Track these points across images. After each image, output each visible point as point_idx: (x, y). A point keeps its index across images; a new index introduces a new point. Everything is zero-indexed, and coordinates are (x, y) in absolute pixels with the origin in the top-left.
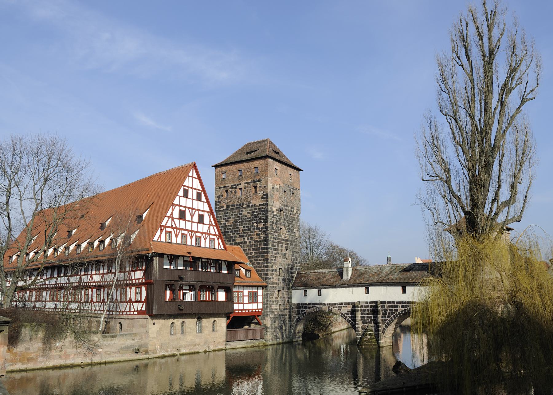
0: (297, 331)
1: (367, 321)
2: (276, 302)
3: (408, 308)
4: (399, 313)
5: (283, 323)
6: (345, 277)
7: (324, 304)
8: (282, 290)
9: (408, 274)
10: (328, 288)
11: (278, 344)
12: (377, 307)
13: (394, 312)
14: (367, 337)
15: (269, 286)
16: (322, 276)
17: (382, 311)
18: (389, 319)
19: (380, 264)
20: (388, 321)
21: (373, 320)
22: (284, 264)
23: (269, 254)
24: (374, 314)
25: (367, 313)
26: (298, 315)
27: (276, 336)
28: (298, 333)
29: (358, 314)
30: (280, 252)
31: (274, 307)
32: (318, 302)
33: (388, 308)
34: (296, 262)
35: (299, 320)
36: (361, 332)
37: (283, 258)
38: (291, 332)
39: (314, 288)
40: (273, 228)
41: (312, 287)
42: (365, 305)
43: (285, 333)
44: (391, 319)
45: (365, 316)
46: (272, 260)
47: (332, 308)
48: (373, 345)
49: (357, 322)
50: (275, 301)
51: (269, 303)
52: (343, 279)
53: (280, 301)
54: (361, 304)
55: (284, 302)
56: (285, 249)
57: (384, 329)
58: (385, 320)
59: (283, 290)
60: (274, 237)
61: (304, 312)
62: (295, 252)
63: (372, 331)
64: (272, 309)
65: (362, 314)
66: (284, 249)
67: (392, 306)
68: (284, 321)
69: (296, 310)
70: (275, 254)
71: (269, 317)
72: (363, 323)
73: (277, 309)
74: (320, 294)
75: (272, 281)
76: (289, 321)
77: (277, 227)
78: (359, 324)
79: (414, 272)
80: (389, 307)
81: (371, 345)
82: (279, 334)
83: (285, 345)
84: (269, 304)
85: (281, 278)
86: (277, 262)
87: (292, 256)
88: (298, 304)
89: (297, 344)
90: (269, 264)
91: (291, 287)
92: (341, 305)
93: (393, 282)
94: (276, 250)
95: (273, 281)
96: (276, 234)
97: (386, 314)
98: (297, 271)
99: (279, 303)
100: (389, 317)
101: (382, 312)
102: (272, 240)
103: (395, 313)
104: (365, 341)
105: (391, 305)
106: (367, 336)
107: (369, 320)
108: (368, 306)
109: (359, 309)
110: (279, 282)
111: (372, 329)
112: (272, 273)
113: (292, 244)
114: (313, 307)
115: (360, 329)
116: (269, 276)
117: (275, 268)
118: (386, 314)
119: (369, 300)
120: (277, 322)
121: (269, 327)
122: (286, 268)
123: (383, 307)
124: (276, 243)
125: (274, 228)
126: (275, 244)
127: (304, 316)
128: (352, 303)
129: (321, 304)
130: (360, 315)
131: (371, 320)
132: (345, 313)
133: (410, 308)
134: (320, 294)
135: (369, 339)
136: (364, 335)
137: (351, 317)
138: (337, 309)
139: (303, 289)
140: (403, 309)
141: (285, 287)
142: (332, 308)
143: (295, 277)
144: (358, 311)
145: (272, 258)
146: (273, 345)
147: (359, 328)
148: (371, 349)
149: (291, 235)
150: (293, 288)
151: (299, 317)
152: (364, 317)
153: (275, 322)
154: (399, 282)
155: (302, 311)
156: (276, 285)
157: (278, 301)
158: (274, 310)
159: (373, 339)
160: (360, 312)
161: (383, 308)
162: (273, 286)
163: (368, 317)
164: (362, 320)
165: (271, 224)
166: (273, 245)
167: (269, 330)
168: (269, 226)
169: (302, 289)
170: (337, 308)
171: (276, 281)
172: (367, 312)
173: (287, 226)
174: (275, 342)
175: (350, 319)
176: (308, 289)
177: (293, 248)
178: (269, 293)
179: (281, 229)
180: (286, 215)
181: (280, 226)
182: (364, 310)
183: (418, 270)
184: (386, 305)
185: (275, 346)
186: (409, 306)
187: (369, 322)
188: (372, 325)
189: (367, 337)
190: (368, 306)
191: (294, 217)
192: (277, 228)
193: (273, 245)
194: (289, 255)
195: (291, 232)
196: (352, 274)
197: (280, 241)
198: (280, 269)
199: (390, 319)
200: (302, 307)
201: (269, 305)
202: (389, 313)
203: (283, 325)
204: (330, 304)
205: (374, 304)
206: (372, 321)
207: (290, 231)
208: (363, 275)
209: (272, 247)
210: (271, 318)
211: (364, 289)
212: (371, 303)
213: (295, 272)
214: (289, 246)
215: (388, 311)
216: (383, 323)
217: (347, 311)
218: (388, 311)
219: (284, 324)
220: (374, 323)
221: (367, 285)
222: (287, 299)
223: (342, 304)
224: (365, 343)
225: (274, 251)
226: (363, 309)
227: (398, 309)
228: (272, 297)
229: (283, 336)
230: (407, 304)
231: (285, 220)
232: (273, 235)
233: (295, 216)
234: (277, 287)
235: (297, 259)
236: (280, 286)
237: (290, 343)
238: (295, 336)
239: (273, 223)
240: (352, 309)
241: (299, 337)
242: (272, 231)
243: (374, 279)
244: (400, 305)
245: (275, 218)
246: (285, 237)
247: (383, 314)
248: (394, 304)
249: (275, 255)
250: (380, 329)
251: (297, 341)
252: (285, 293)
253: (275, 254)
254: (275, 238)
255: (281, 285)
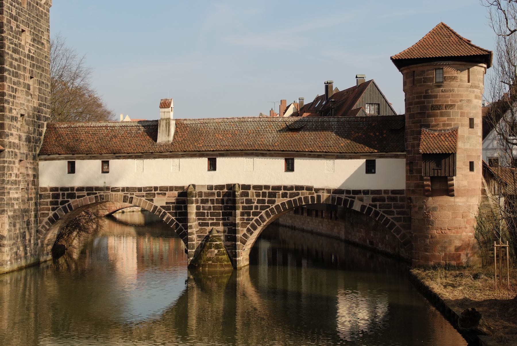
0: (46, 242)
1: (210, 222)
2: (16, 184)
3: (297, 198)
4: (277, 207)
5: (26, 226)
6: (163, 138)
7: (114, 190)
8: (25, 159)
9: (297, 135)
10: (125, 157)
11: (20, 269)
12: (235, 196)
13: (266, 204)
14: (211, 252)
15: (6, 150)
16: (107, 135)
17: (243, 203)
18: (255, 218)
19: (235, 117)
20: (253, 221)
21: (223, 219)
22: (27, 106)
23: (5, 83)
24: (225, 208)
25: (210, 207)
26: (53, 209)
27: (16, 253)
28: (48, 245)
29: (192, 209)
30: (22, 81)
31: (14, 194)
32: (100, 184)
33: (255, 197)
34: (45, 105)
35: (53, 221)
36: (195, 241)
37: (28, 94)
38: (38, 244)
39: (91, 158)
40: (11, 28)
41: (90, 155)
42: (206, 190)
43: (30, 245)
44: (261, 217)
45: (206, 211)
46: (10, 95)
47: (134, 196)
48: (226, 265)
49: (189, 224)
50: (15, 183)
51: (5, 186)
52: (158, 141)
53: (22, 183)
54: (197, 190)
55: (28, 185)
56: (29, 75)
57: (244, 235)
58: (248, 220)
59: (27, 159)
60: (13, 48)
61: (67, 204)
62: (43, 83)
63: (220, 240)
64: (10, 199)
65: (198, 208)
66: (28, 75)
67: (264, 195)
68: (28, 223)
69: (49, 200)
70: (14, 83)
71: (6, 215)
72: (200, 224)
73: (17, 199)
74: (105, 171)
75: (10, 140)
76: (34, 221)
77: (18, 26)
78: (193, 226)
79: (307, 133)
80: (258, 195)
81: (222, 266)
82: (21, 248)
83: (29, 270)
84: (6, 188)
85: (24, 136)
86: (17, 101)
87: (40, 89)
88: (53, 189)
89: (45, 266)
90: (6, 105)
91: (39, 155)
92: (153, 192)
93: (269, 150)
94: (16, 75)
95: (12, 141)
96: (15, 41)
97: (251, 208)
98: (45, 123)
99: (21, 187)
100: (255, 214)
101: (241, 205)
102: (10, 52)
103: (269, 207)
104: (209, 259)
105: (261, 192)
106: (213, 249)
107: (213, 219)
108: (213, 194)
109: (194, 198)
110: (21, 143)
111: (220, 236)
112: (10, 123)
113: (40, 67)
114: (88, 194)
115: (195, 236)
116: (6, 130)
117: (14, 113)
118: (251, 208)
119: (215, 183)
120: (18, 226)
121: (5, 236)
122: (31, 114)
123: (245, 196)
124: (16, 60)
125: (14, 29)
126: (15, 63)
127: (66, 212)
128: (177, 188)
129: (108, 188)
130: (195, 211)
131: (217, 219)
132: (161, 207)
133: (300, 199)
134: (105, 171)
135: (216, 254)
136: (203, 248)
137: (175, 214)
138: (143, 199)
139: (66, 158)
140: (285, 200)
141: (29, 154)
142: (132, 198)
143: (43, 134)
144: (192, 203)
145: (11, 93)
146: (13, 271)
147: (194, 234)
148: (222, 273)
149: (38, 47)
150: (43, 157)
151: (55, 215)
152: (203, 214)
153: (15, 226)
154: (283, 151)
155: (63, 203)
156: (16, 150)
157: (19, 181)
158: (13, 202)
159: (224, 254)
160: (194, 205)
161: (245, 198)
162: (12, 152)
163: (212, 214)
164: (199, 219)
165: (9, 18)
166: (11, 65)
167: (6, 242)
168: (5, 21)
169: (63, 159)
170: (143, 196)
171: (17, 141)
172: (209, 204)
173: (32, 28)
174: (15, 266)
175: (174, 218)
176: (79, 158)
177: (41, 75)
178: (6, 165)
179: (23, 31)
180: (30, 3)
181: (22, 27)
182: (204, 201)
183: (316, 130)
184: (251, 191)
185: (16, 274)
186: (298, 194)
187: (212, 224)
188: (221, 228)
189: (211, 252)
190: (213, 194)
191: (42, 12)
192: (17, 29)
193: (11, 65)
194: (34, 88)
195: (39, 42)
196: (176, 132)
197: (22, 58)
198: (22, 115)
199: (258, 217)
200: (63, 195)
201: (6, 191)
202: (256, 207)
203: (26, 230)
204: (128, 189)
205: (225, 190)
206: (221, 222)
207: (36, 40)
208: (201, 134)
209: (11, 69)
210: (9, 217)
211: (204, 161)
212: (221, 187)
213: (43, 124)
214: (35, 70)
215: (256, 204)
216: (244, 225)
217: (167, 203)
218: (256, 204)
219: (28, 229)
220: (224, 225)
221: (212, 155)
222: (32, 179)
223: (156, 188)
224: (210, 262)
225: (13, 78)
226: (202, 200)
227: (276, 199)
228: (11, 174)
229: (26, 253)
230: (294, 191)
231: (29, 14)
232: (12, 43)
233: (44, 8)
234: (18, 154)
235: (46, 98)
236: (22, 151)
237: (36, 265)
238: (43, 251)
239: (11, 16)
240: (177, 199)
241: (48, 254)
242: (10, 35)
243: (226, 144)
244: (281, 192)
245: (14, 7)
246: (29, 51)
247: (244, 208)
248: (267, 191)
249: (15, 87)
250: (239, 235)
251: (46, 261)
252: (29, 165)
253: (14, 83)
254: (15, 51)
255: (24, 150)
